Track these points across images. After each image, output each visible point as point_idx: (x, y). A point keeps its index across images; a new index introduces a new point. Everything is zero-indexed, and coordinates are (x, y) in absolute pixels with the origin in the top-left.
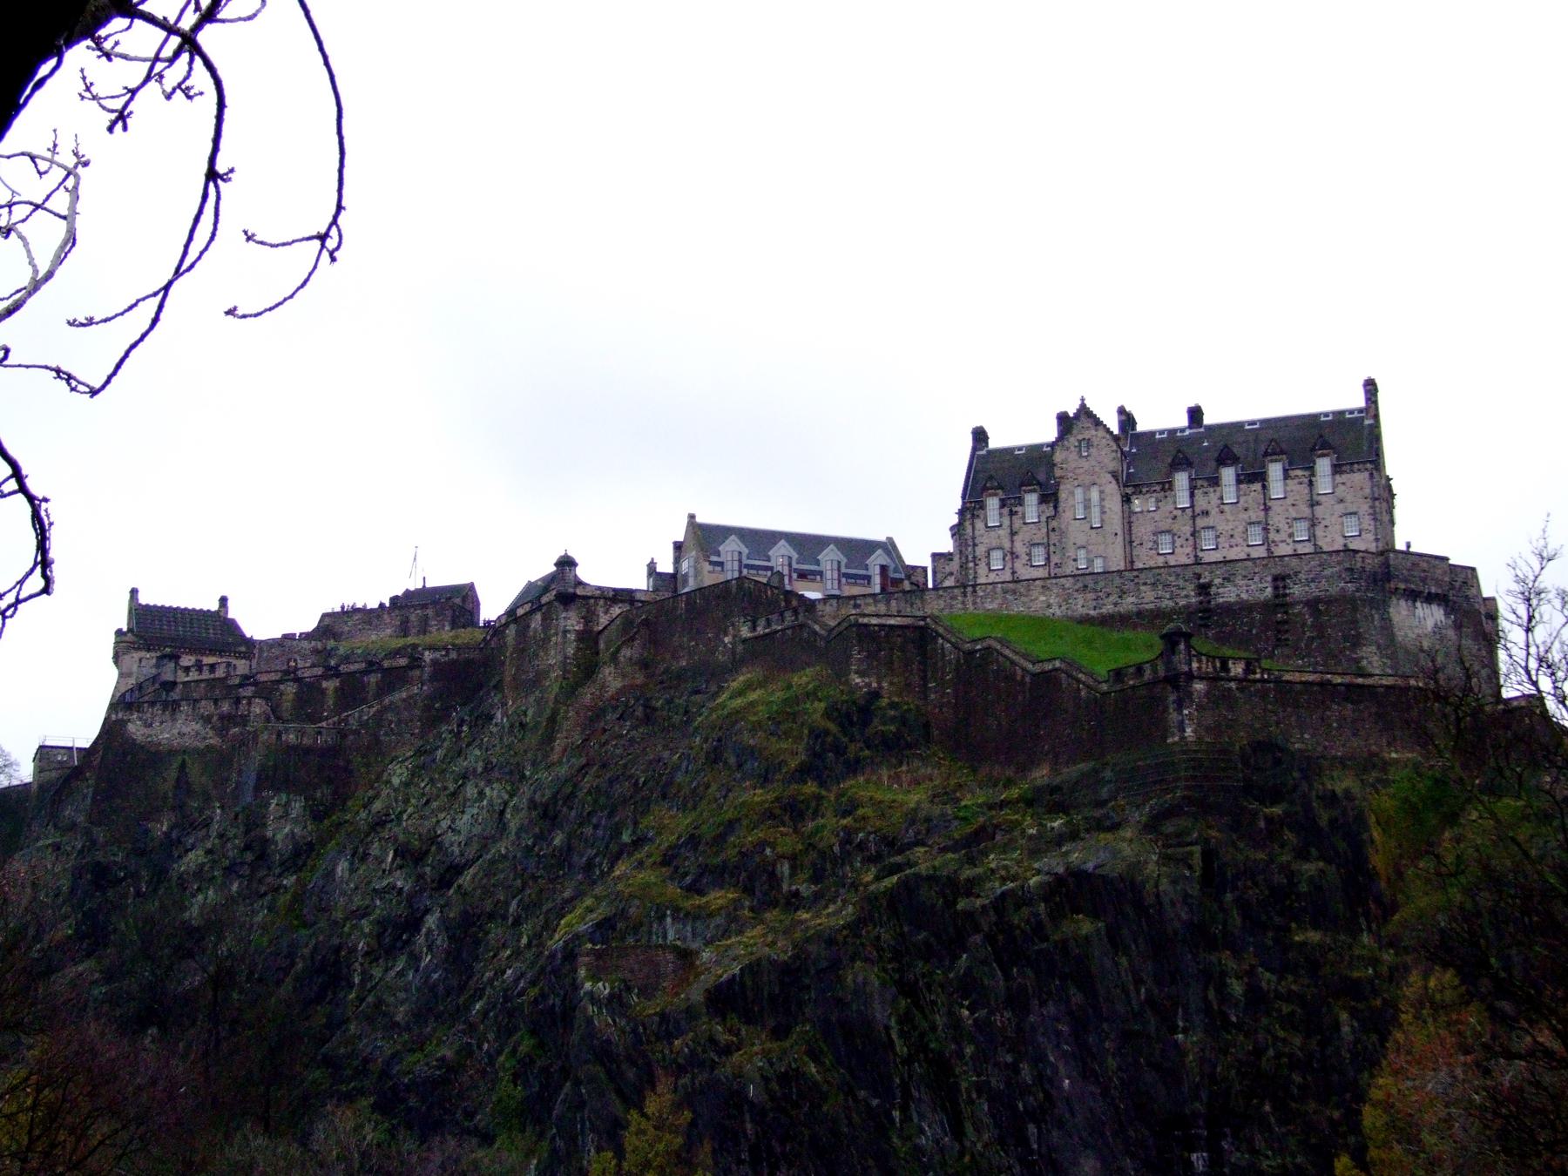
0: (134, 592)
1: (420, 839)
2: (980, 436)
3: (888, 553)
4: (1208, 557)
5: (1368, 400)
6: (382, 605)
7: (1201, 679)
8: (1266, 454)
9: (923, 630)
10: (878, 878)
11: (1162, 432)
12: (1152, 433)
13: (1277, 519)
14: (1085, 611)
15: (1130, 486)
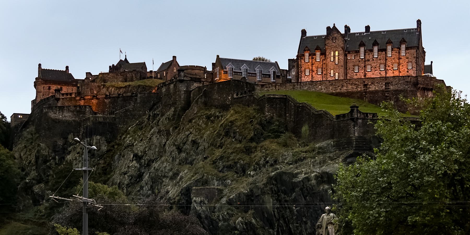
0: (40, 65)
1: (141, 152)
2: (304, 32)
3: (275, 67)
4: (369, 75)
5: (417, 26)
6: (113, 65)
7: (361, 119)
8: (387, 43)
9: (286, 99)
10: (272, 172)
11: (357, 33)
12: (355, 34)
13: (389, 63)
14: (331, 91)
15: (346, 52)
